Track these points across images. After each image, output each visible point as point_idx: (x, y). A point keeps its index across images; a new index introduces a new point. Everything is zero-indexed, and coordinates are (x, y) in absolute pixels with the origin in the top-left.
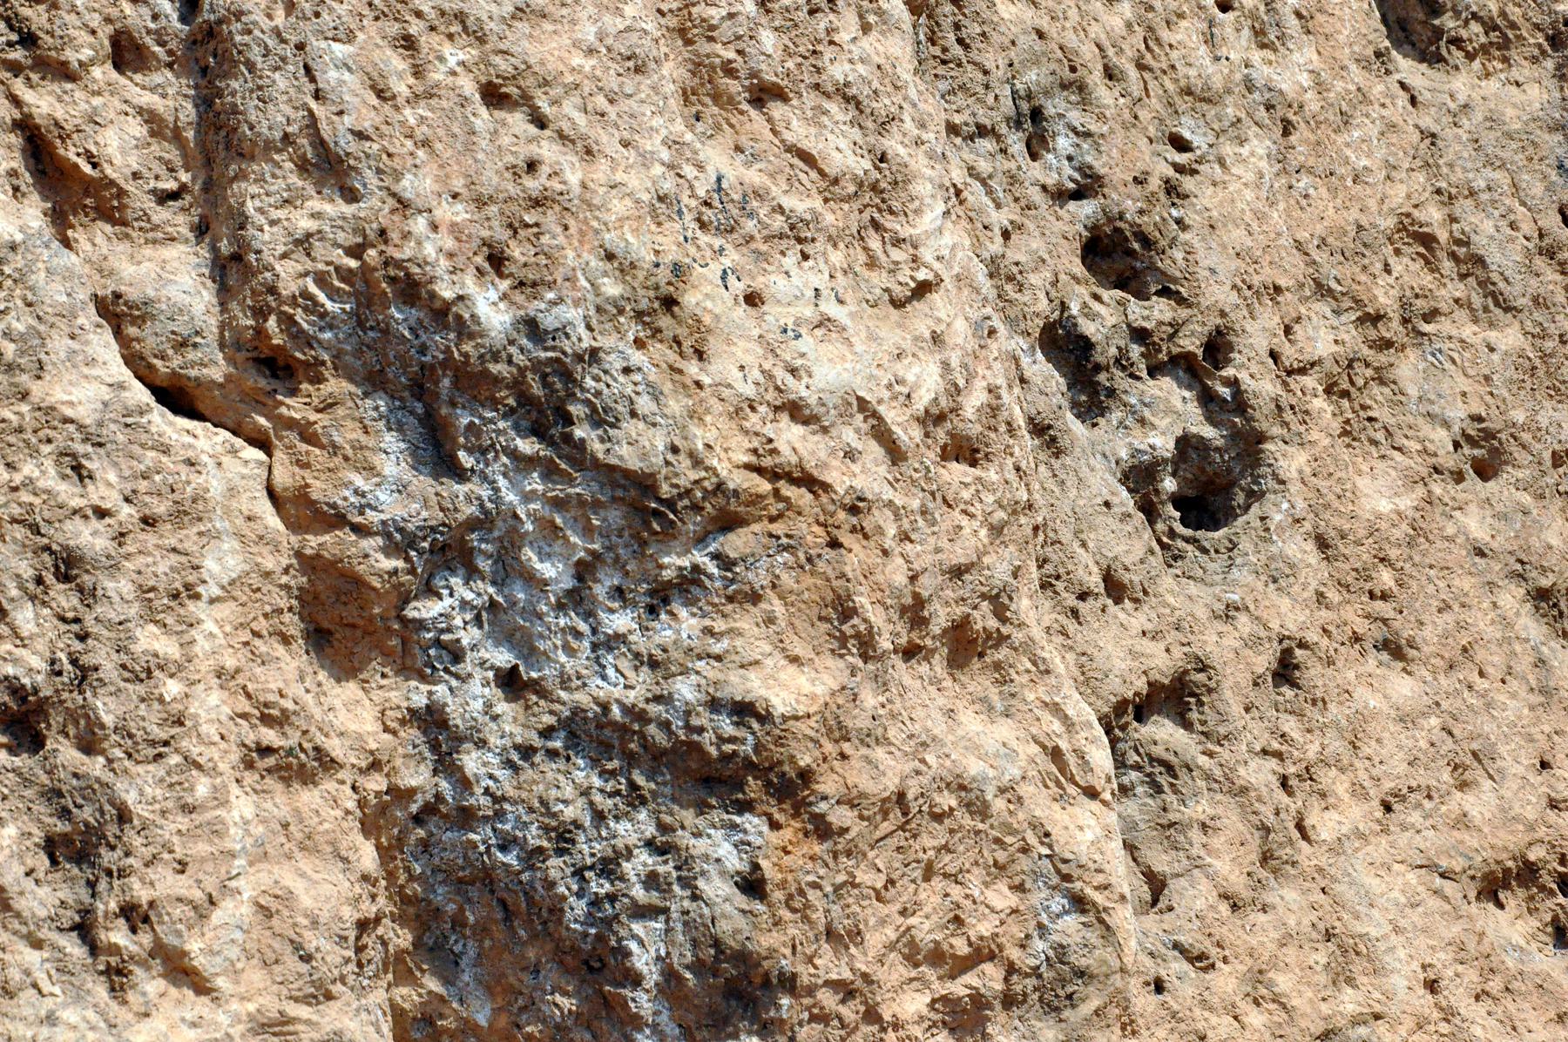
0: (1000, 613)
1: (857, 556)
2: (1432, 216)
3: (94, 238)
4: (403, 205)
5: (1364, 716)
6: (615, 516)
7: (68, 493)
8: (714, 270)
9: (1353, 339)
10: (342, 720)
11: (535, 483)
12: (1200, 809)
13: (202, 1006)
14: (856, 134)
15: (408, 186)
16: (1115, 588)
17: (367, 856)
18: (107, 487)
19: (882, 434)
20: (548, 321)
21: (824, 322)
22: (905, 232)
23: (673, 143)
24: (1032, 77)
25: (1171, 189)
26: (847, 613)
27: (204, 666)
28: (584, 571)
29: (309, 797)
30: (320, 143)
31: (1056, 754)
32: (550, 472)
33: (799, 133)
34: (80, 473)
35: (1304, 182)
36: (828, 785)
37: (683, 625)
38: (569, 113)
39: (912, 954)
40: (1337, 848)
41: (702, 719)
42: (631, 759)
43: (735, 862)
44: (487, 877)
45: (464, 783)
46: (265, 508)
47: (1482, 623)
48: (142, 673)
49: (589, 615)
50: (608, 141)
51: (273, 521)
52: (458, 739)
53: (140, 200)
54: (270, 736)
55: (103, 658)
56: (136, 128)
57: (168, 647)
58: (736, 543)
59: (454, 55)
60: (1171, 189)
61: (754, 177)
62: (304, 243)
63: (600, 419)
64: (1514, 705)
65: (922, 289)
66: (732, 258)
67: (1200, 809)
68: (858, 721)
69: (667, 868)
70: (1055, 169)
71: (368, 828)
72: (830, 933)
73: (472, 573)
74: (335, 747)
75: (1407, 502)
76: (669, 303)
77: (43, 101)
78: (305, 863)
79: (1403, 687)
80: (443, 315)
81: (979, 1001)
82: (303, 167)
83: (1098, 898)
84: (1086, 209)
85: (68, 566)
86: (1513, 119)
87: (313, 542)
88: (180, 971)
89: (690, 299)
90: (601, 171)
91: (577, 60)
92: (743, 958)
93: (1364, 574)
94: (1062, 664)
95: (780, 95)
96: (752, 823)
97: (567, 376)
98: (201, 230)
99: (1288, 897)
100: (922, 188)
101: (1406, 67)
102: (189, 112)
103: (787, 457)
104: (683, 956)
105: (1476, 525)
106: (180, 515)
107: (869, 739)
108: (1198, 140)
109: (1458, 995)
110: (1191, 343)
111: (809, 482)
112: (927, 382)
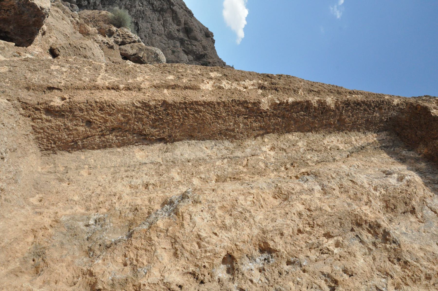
8: (203, 207)
14: (231, 224)
83: (147, 276)
89: (198, 204)
103: (184, 215)
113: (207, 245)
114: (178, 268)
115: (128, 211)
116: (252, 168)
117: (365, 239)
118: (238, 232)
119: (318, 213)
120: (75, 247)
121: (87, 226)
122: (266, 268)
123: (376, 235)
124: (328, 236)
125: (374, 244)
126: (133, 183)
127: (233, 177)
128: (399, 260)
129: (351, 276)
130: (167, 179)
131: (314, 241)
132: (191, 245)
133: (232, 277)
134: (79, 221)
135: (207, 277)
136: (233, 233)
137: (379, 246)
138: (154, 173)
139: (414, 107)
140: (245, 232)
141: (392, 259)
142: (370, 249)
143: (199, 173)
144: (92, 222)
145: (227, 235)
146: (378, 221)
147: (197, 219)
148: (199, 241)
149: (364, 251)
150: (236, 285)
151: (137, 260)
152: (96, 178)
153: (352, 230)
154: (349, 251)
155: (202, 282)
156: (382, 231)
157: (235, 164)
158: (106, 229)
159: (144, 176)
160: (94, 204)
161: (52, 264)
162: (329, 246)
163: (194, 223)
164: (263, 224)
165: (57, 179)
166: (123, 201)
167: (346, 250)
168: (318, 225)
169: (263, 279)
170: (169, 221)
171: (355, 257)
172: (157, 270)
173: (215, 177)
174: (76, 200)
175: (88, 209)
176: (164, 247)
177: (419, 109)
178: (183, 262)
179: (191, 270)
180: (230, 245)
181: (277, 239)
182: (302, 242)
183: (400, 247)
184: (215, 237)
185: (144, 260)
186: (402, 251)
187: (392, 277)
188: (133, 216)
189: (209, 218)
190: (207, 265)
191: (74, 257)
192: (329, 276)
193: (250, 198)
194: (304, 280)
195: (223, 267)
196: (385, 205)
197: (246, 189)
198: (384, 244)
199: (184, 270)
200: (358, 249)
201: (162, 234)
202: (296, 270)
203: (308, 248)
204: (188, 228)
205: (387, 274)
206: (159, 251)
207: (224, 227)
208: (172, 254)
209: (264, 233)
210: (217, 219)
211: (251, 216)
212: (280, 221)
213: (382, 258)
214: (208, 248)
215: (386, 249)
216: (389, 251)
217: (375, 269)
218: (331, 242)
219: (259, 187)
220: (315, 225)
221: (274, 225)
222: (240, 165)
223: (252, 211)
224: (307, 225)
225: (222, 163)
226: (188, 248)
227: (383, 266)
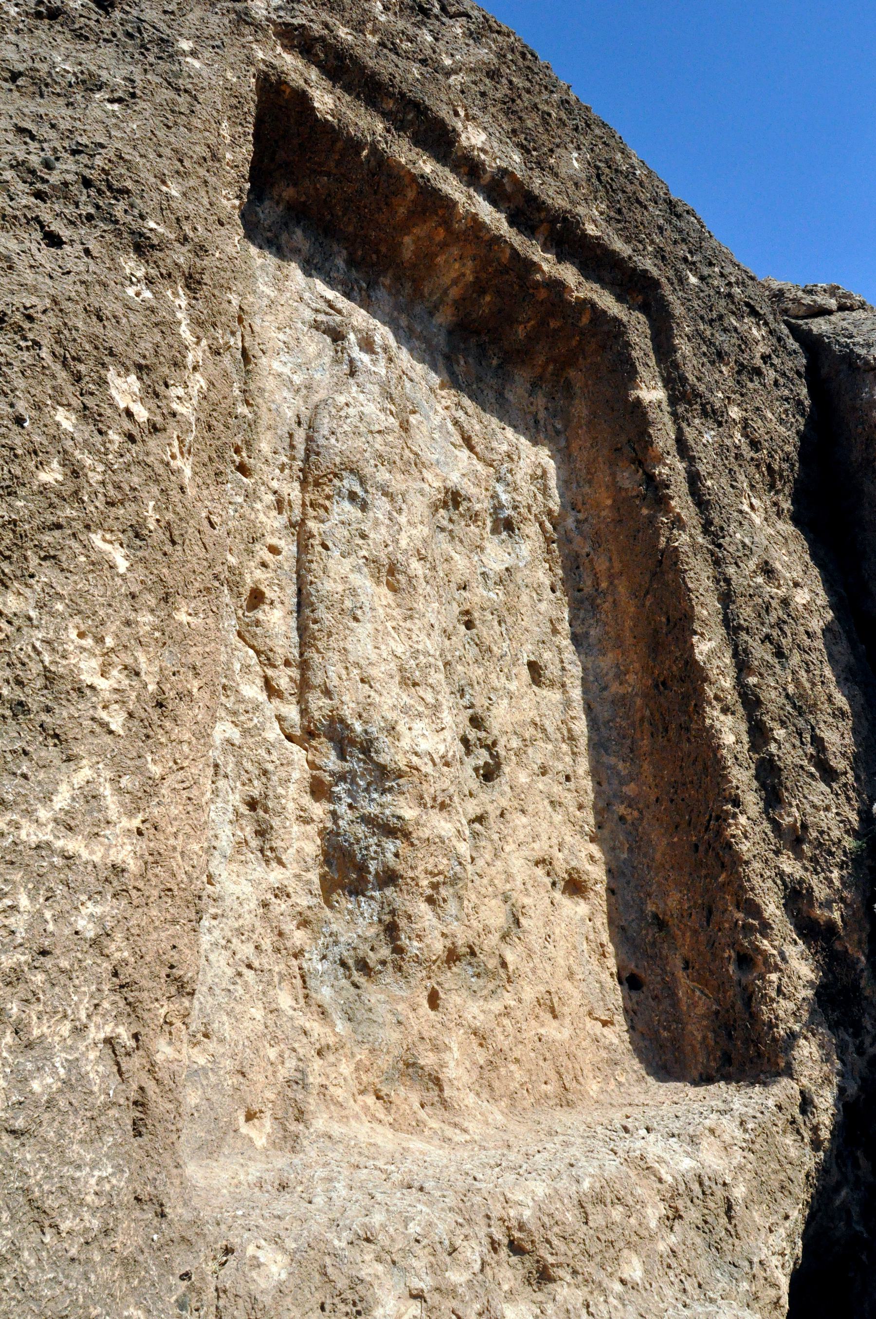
0: (451, 800)
1: (425, 786)
2: (537, 719)
3: (276, 702)
4: (342, 702)
5: (516, 826)
6: (377, 773)
7: (267, 757)
9: (520, 743)
10: (316, 811)
11: (361, 764)
12: (483, 843)
13: (283, 870)
15: (344, 698)
16: (471, 795)
17: (319, 842)
18: (274, 757)
19: (432, 760)
20: (369, 731)
21: (423, 735)
23: (398, 694)
24: (463, 682)
25: (488, 708)
26: (422, 798)
27: (290, 797)
28: (369, 784)
29: (308, 827)
30: (326, 688)
31: (459, 831)
32: (365, 763)
33: (421, 693)
34: (269, 752)
36: (414, 835)
37: (388, 798)
38: (377, 686)
39: (426, 872)
40: (509, 854)
41: (391, 818)
42: (374, 826)
43: (393, 850)
44: (341, 848)
45: (339, 827)
46: (305, 764)
47: (541, 807)
48: (278, 797)
49: (369, 794)
50: (385, 692)
51: (307, 767)
52: (339, 818)
53: (286, 695)
54: (302, 814)
55: (271, 793)
56: (287, 679)
57: (283, 792)
58: (401, 781)
59: (356, 671)
60: (488, 708)
61: (412, 702)
62: (320, 708)
63: (377, 752)
64: (545, 825)
65: (443, 729)
66: (407, 719)
67: (483, 843)
68: (422, 822)
69: (379, 850)
70: (465, 702)
71: (319, 835)
72: (411, 867)
73: (346, 782)
74: (315, 817)
75: (528, 780)
76: (393, 728)
77: (270, 672)
78: (307, 842)
79: (524, 820)
80: (348, 727)
81: (438, 883)
82: (322, 692)
84: (471, 711)
85: (265, 772)
87: (315, 772)
88: (280, 862)
89: (398, 728)
90: (383, 699)
92: (393, 871)
94: (460, 810)
95: (418, 685)
96: (398, 841)
97: (372, 742)
98: (298, 702)
99: (498, 863)
100: (444, 707)
101: (534, 688)
102: (298, 677)
104: (380, 869)
105: (541, 786)
106: (289, 764)
107: (424, 826)
109: (529, 886)
110: (489, 742)
111: (417, 769)
112: (442, 749)
129: (464, 588)
137: (455, 517)
139: (271, 84)
142: (451, 531)
177: (287, 95)
215: (462, 515)
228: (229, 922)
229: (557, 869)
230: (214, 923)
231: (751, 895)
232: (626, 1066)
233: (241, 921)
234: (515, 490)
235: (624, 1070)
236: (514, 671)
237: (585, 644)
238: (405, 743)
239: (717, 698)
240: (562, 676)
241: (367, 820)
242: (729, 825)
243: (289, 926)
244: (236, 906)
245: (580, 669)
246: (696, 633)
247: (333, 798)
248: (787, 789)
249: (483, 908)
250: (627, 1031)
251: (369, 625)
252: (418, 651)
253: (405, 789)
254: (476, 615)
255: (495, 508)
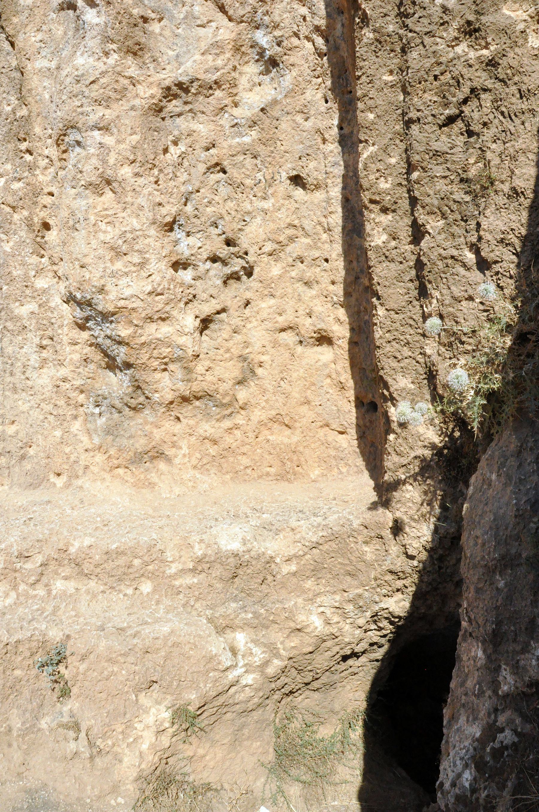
2: (296, 222)
22: (148, 267)
28: (102, 320)
35: (268, 222)
37: (113, 325)
38: (90, 268)
40: (250, 329)
47: (290, 291)
50: (93, 271)
58: (116, 316)
59: (77, 263)
65: (150, 275)
67: (224, 327)
70: (219, 231)
77: (55, 268)
84: (224, 236)
85: (52, 324)
86: (316, 202)
89: (106, 288)
90: (92, 275)
91: (91, 261)
93: (269, 285)
103: (119, 306)
105: (293, 274)
106: (62, 317)
108: (248, 220)
113: (162, 287)
114: (181, 318)
115: (87, 369)
116: (22, 202)
117: (178, 110)
118: (151, 251)
119: (139, 154)
120: (131, 424)
121: (100, 414)
122: (188, 230)
123: (176, 96)
124: (166, 151)
125: (186, 103)
126: (37, 365)
127: (36, 232)
128: (211, 88)
129: (214, 146)
130: (34, 321)
131: (170, 171)
132: (158, 302)
133: (192, 266)
134: (96, 425)
135: (191, 290)
136: (152, 258)
137: (189, 99)
138: (20, 338)
140: (152, 244)
141: (208, 95)
142: (191, 111)
143: (26, 277)
144: (97, 410)
145: (153, 265)
146: (163, 86)
147: (127, 292)
148: (154, 294)
149: (190, 118)
150: (200, 264)
151: (164, 358)
152: (23, 412)
153: (163, 119)
154: (186, 134)
155: (194, 296)
156: (175, 88)
157: (10, 223)
158: (110, 393)
159: (24, 350)
160: (68, 411)
161: (154, 443)
162: (176, 154)
163: (132, 296)
164: (145, 221)
165: (20, 462)
166: (70, 376)
167: (184, 137)
168: (154, 160)
169: (199, 235)
170: (122, 323)
171: (194, 132)
172: (179, 338)
173: (34, 256)
174: (61, 433)
175: (76, 417)
176: (154, 331)
178: (175, 313)
179: (183, 306)
180: (164, 263)
181: (164, 211)
182: (170, 184)
183: (200, 80)
184: (153, 277)
185: (165, 351)
186: (204, 80)
187: (226, 106)
188: (93, 364)
189: (128, 279)
190: (181, 290)
191: (146, 422)
192: (208, 169)
193: (103, 226)
194: (208, 196)
195: (181, 272)
196: (131, 55)
197: (86, 227)
198: (190, 94)
199: (183, 312)
200: (186, 124)
201: (139, 331)
202: (195, 199)
203: (176, 179)
204: (137, 304)
205: (222, 109)
206: (159, 336)
207: (142, 265)
208: (162, 323)
209: (154, 223)
210: (130, 271)
211: (131, 232)
212: (141, 201)
213: (205, 104)
214: (166, 286)
215: (195, 94)
216: (200, 93)
217: (214, 119)
218: (172, 149)
219: (86, 210)
220: (154, 162)
221: (147, 210)
222: (12, 217)
223: (123, 229)
224: (152, 171)
225: (6, 241)
226: (160, 306)
227: (213, 109)
228: (38, 397)
229: (302, 332)
230: (31, 398)
231: (381, 373)
232: (350, 462)
233: (44, 396)
234: (276, 26)
235: (346, 464)
236: (270, 191)
237: (349, 143)
238: (112, 296)
239: (372, 201)
240: (325, 179)
241: (109, 337)
242: (374, 316)
243: (73, 395)
244: (41, 389)
245: (342, 168)
246: (361, 142)
247: (90, 329)
248: (430, 282)
249: (218, 368)
250: (357, 439)
251: (83, 231)
252: (126, 231)
253: (119, 320)
254: (225, 163)
255: (258, 54)
